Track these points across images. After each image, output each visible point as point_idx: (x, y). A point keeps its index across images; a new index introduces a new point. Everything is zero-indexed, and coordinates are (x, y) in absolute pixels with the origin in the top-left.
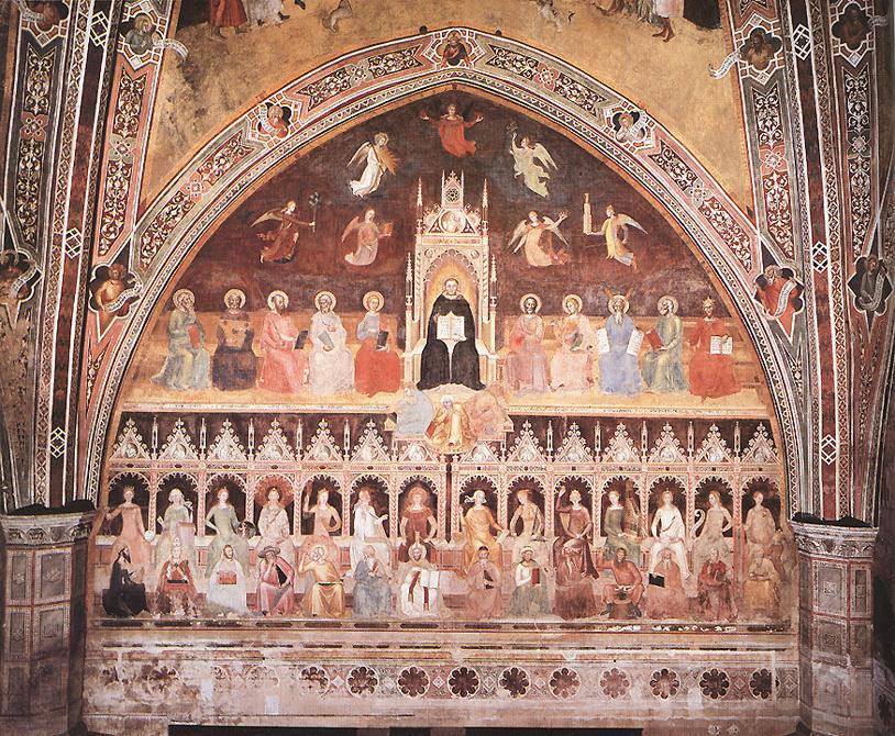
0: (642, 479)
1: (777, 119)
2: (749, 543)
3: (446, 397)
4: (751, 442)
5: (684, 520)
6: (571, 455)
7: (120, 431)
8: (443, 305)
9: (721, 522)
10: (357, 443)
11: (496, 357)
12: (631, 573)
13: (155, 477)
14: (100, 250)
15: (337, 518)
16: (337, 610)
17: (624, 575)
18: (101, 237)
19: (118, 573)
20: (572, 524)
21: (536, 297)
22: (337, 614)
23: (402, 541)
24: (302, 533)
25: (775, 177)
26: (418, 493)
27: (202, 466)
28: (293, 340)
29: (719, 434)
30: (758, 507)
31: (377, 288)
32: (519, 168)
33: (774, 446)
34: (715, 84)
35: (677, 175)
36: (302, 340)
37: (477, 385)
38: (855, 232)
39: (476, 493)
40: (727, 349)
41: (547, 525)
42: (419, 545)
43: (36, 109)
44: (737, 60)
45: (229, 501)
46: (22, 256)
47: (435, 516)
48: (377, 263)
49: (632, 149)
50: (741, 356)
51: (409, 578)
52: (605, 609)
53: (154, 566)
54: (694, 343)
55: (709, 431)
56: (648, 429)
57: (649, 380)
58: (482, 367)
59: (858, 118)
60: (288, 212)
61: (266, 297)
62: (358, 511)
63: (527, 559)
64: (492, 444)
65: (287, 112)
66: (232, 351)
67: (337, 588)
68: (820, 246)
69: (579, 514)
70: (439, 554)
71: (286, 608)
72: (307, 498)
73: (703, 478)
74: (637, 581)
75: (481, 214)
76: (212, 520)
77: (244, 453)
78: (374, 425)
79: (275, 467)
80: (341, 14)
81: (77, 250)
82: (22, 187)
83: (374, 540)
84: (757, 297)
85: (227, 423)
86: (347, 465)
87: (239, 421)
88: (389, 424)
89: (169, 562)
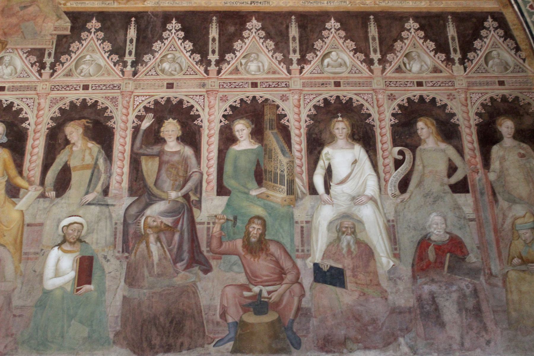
0: (293, 98)
2: (503, 204)
5: (375, 166)
6: (166, 66)
9: (443, 168)
12: (277, 262)
20: (164, 175)
29: (422, 34)
30: (508, 141)
33: (517, 49)
41: (115, 178)
52: (224, 332)
56: (300, 27)
64: (31, 52)
69: (176, 158)
73: (402, 98)
74: (289, 277)
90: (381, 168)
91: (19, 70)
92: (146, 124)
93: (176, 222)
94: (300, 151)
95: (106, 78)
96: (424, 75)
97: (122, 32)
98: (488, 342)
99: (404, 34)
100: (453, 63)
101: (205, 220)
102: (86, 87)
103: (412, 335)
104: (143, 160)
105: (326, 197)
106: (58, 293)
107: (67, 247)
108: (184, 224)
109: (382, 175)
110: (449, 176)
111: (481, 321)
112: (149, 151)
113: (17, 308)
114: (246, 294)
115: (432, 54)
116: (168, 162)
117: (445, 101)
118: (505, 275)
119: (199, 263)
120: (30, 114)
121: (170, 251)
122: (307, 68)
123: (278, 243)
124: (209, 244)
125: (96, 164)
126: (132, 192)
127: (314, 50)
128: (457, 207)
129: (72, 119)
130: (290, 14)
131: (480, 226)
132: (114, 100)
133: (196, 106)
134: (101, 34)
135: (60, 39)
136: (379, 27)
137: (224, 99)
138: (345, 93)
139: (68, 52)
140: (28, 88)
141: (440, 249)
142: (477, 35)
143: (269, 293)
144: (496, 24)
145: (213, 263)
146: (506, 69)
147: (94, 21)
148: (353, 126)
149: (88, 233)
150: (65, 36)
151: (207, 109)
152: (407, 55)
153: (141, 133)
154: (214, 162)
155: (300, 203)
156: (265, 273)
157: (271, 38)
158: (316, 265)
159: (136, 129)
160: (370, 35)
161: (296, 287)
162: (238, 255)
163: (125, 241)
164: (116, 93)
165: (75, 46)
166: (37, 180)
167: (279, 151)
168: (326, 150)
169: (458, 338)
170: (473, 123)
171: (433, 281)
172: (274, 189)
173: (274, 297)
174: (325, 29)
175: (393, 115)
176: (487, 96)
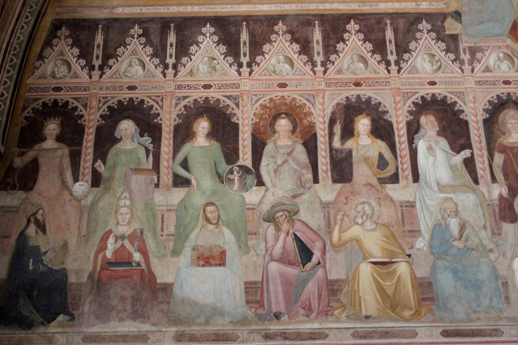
7: (48, 43)
10: (407, 51)
13: (94, 103)
15: (388, 155)
16: (407, 307)
22: (407, 313)
24: (335, 181)
45: (212, 134)
53: (86, 238)
62: (421, 146)
71: (315, 305)
72: (338, 129)
76: (185, 164)
77: (235, 67)
78: (429, 27)
79: (283, 85)
83: (453, 188)
85: (208, 29)
89: (110, 232)
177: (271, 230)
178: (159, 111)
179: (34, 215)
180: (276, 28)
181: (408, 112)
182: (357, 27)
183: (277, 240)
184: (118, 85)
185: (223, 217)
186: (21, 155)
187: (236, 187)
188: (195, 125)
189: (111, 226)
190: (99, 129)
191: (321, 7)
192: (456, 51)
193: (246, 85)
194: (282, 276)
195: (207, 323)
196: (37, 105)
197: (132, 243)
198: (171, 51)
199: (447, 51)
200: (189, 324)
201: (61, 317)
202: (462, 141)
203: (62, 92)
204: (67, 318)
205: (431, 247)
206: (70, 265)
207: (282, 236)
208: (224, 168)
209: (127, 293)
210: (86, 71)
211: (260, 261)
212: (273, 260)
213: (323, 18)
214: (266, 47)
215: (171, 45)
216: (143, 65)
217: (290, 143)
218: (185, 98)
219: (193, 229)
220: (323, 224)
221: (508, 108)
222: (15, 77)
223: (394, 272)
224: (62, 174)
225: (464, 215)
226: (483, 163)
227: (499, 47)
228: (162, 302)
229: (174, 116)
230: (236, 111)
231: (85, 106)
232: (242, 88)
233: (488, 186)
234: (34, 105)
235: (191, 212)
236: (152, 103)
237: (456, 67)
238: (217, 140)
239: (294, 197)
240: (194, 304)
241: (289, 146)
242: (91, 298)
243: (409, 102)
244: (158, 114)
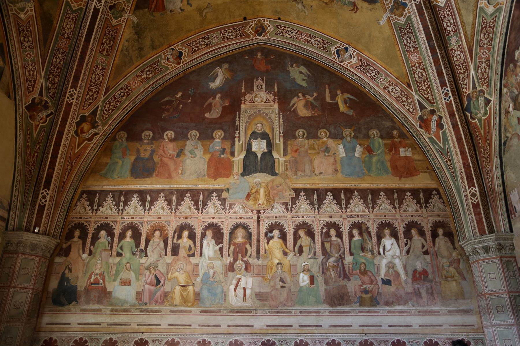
1: (412, 38)
2: (440, 258)
3: (257, 180)
4: (430, 201)
6: (328, 209)
7: (79, 200)
8: (254, 135)
9: (420, 246)
11: (284, 159)
12: (370, 278)
13: (93, 224)
14: (84, 106)
15: (192, 246)
17: (366, 279)
18: (86, 100)
19: (63, 279)
20: (332, 249)
21: (304, 131)
22: (190, 304)
23: (230, 260)
24: (172, 255)
25: (417, 65)
26: (240, 232)
27: (120, 218)
28: (175, 154)
29: (412, 197)
30: (441, 237)
31: (221, 128)
32: (292, 75)
33: (444, 203)
34: (381, 27)
35: (370, 73)
36: (181, 153)
37: (273, 173)
38: (462, 83)
39: (274, 232)
40: (409, 154)
41: (317, 250)
42: (241, 262)
43: (66, 36)
44: (389, 15)
45: (132, 237)
46: (46, 102)
47: (251, 245)
48: (222, 116)
49: (347, 65)
50: (416, 157)
51: (235, 282)
52: (356, 300)
53: (85, 275)
54: (391, 151)
55: (406, 195)
57: (369, 169)
58: (276, 164)
59: (450, 29)
60: (178, 96)
61: (163, 134)
62: (205, 242)
63: (305, 270)
64: (283, 204)
65: (181, 54)
66: (143, 159)
67: (191, 288)
68: (445, 89)
69: (335, 243)
70: (252, 267)
71: (159, 300)
72: (176, 235)
73: (406, 221)
74: (374, 282)
75: (274, 94)
76: (121, 248)
77: (143, 211)
78: (216, 195)
79: (159, 218)
80: (207, 10)
81: (73, 99)
82: (53, 69)
84: (421, 127)
86: (201, 217)
87: (142, 194)
88: (225, 195)
89: (93, 272)
90: (401, 246)
91: (280, 211)
92: (324, 231)
93: (338, 264)
94: (375, 240)
95: (309, 214)
96: (413, 212)
97: (312, 197)
98: (436, 303)
99: (406, 197)
100: (423, 208)
101: (347, 264)
102: (303, 217)
103: (413, 301)
104: (325, 243)
105: (384, 256)
106: (305, 287)
107: (305, 272)
108: (341, 265)
109: (401, 248)
110: (422, 249)
111: (433, 297)
112: (327, 240)
113: (293, 292)
114: (362, 288)
115: (416, 204)
116: (333, 244)
117: (420, 222)
118: (441, 282)
119: (346, 278)
120: (286, 226)
121: (337, 274)
122: (375, 210)
123: (370, 271)
124: (349, 272)
125: (310, 244)
126: (323, 254)
127: (377, 204)
128: (425, 260)
129: (300, 229)
130: (368, 189)
131: (432, 266)
132: (313, 222)
133: (340, 224)
134: (305, 197)
135: (292, 198)
136: (398, 194)
137: (349, 222)
138: (388, 219)
139: (296, 204)
140: (284, 217)
141: (420, 273)
142: (430, 198)
143: (369, 287)
144: (436, 193)
145: (351, 278)
146: (440, 210)
147: (302, 192)
148: (391, 231)
149: (311, 268)
150: (294, 198)
151: (343, 225)
152: (407, 205)
153: (323, 234)
154: (348, 244)
155: (376, 258)
156: (367, 281)
157: (362, 199)
158: (382, 278)
159: (322, 232)
160: (395, 198)
161: (377, 285)
162: (358, 275)
163: (323, 271)
164: (313, 219)
165: (297, 201)
166: (292, 250)
167: (368, 240)
168: (383, 240)
169: (426, 302)
170: (429, 230)
171: (418, 284)
172: (367, 253)
173: (370, 289)
174: (380, 195)
175: (404, 227)
176: (434, 220)
177: (148, 273)
178: (115, 227)
179: (68, 265)
180: (160, 195)
181: (203, 229)
182: (190, 195)
183: (149, 276)
184: (102, 217)
185: (132, 268)
186: (66, 243)
187: (138, 257)
188: (127, 233)
189: (94, 270)
190: (93, 234)
191: (178, 186)
192: (224, 205)
193: (146, 218)
194: (149, 290)
195: (122, 306)
196: (73, 224)
197: (100, 276)
198: (122, 204)
199: (221, 205)
200: (115, 306)
201: (74, 303)
202: (220, 241)
203: (82, 219)
204: (76, 303)
205: (202, 281)
206: (79, 284)
207: (151, 275)
208: (135, 249)
209: (97, 295)
210: (91, 211)
211: (142, 284)
212: (147, 284)
213: (178, 191)
214: (156, 203)
215: (122, 201)
216: (111, 209)
217: (159, 241)
218: (124, 222)
219: (121, 272)
220: (166, 271)
221: (239, 228)
222: (65, 214)
223: (188, 289)
224: (79, 251)
225: (216, 269)
226: (226, 250)
227: (241, 203)
228: (108, 298)
229: (120, 229)
230: (142, 228)
231: (89, 225)
232: (145, 219)
233: (226, 258)
234: (72, 224)
235: (121, 265)
236: (113, 224)
237: (223, 211)
238: (134, 239)
239: (157, 261)
240: (118, 299)
241: (158, 242)
242: (84, 296)
243: (204, 225)
244: (114, 229)
